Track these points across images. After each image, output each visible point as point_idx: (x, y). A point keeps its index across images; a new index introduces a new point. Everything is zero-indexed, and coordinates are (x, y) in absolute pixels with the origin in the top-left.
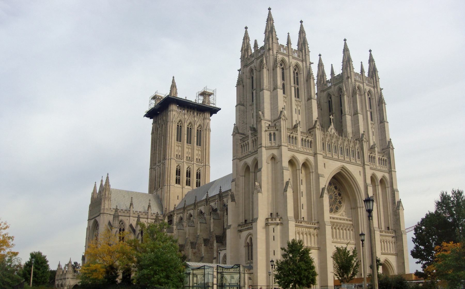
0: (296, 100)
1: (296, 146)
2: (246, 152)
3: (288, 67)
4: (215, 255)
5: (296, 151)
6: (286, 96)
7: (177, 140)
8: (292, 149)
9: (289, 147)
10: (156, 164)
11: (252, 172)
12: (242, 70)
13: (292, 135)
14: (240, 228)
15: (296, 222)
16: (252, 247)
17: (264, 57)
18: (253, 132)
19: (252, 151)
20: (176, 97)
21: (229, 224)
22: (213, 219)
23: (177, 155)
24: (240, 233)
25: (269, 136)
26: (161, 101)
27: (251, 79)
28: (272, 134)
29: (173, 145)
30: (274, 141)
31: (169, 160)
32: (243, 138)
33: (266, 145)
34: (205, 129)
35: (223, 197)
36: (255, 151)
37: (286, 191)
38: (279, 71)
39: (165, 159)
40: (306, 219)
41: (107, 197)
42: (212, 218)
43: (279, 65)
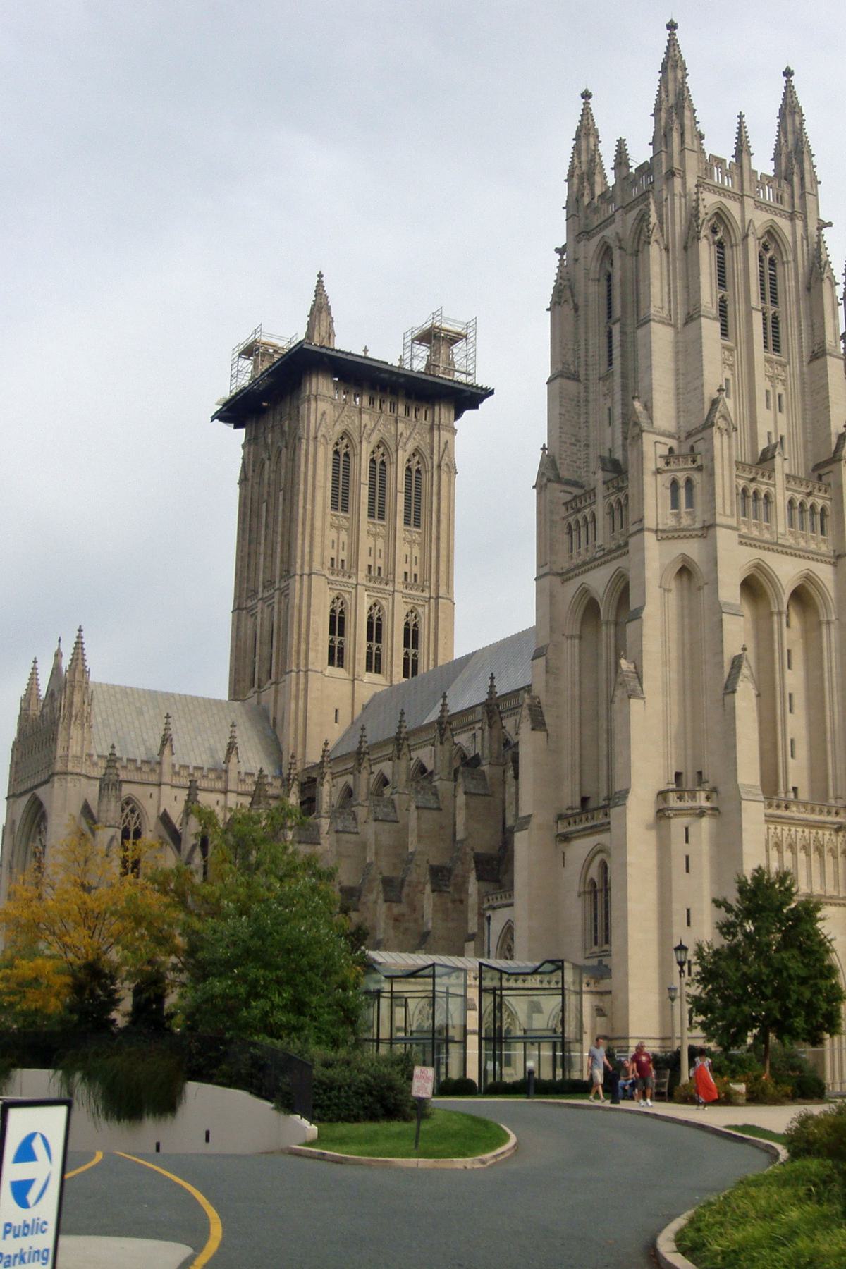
0: (768, 360)
1: (767, 528)
2: (587, 550)
3: (739, 236)
4: (473, 927)
5: (766, 546)
6: (730, 344)
7: (335, 506)
8: (755, 540)
9: (744, 530)
10: (256, 592)
11: (607, 623)
12: (570, 250)
13: (753, 486)
14: (563, 828)
15: (770, 806)
16: (607, 895)
17: (651, 200)
18: (610, 476)
19: (607, 547)
20: (327, 348)
21: (522, 814)
22: (466, 793)
23: (332, 559)
24: (562, 846)
25: (669, 492)
26: (274, 364)
27: (604, 282)
28: (682, 483)
29: (318, 524)
30: (687, 507)
31: (305, 577)
32: (576, 497)
33: (657, 524)
34: (435, 463)
35: (500, 713)
36: (619, 547)
37: (734, 691)
38: (706, 253)
39: (288, 573)
40: (804, 795)
41: (76, 716)
42: (460, 791)
43: (705, 231)
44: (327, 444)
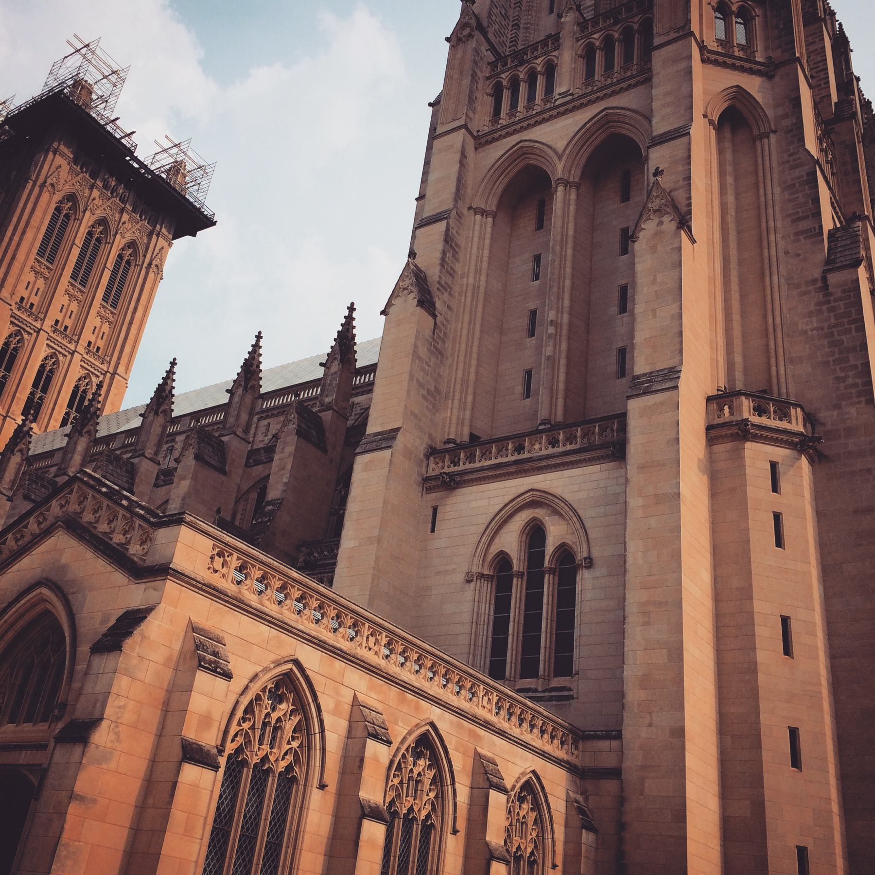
7: (41, 252)
29: (21, 256)
34: (147, 261)
44: (54, 193)
